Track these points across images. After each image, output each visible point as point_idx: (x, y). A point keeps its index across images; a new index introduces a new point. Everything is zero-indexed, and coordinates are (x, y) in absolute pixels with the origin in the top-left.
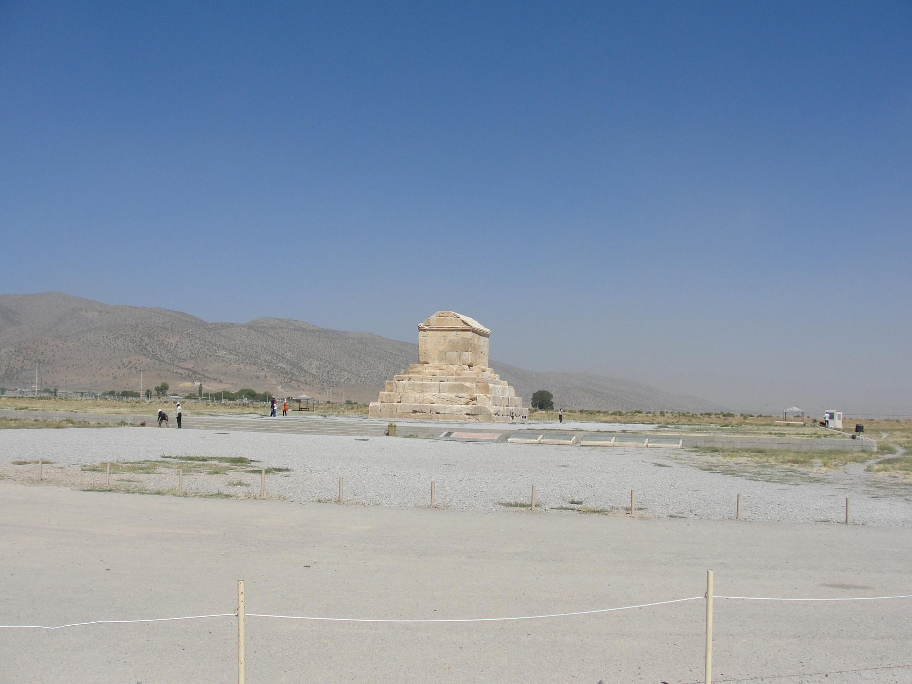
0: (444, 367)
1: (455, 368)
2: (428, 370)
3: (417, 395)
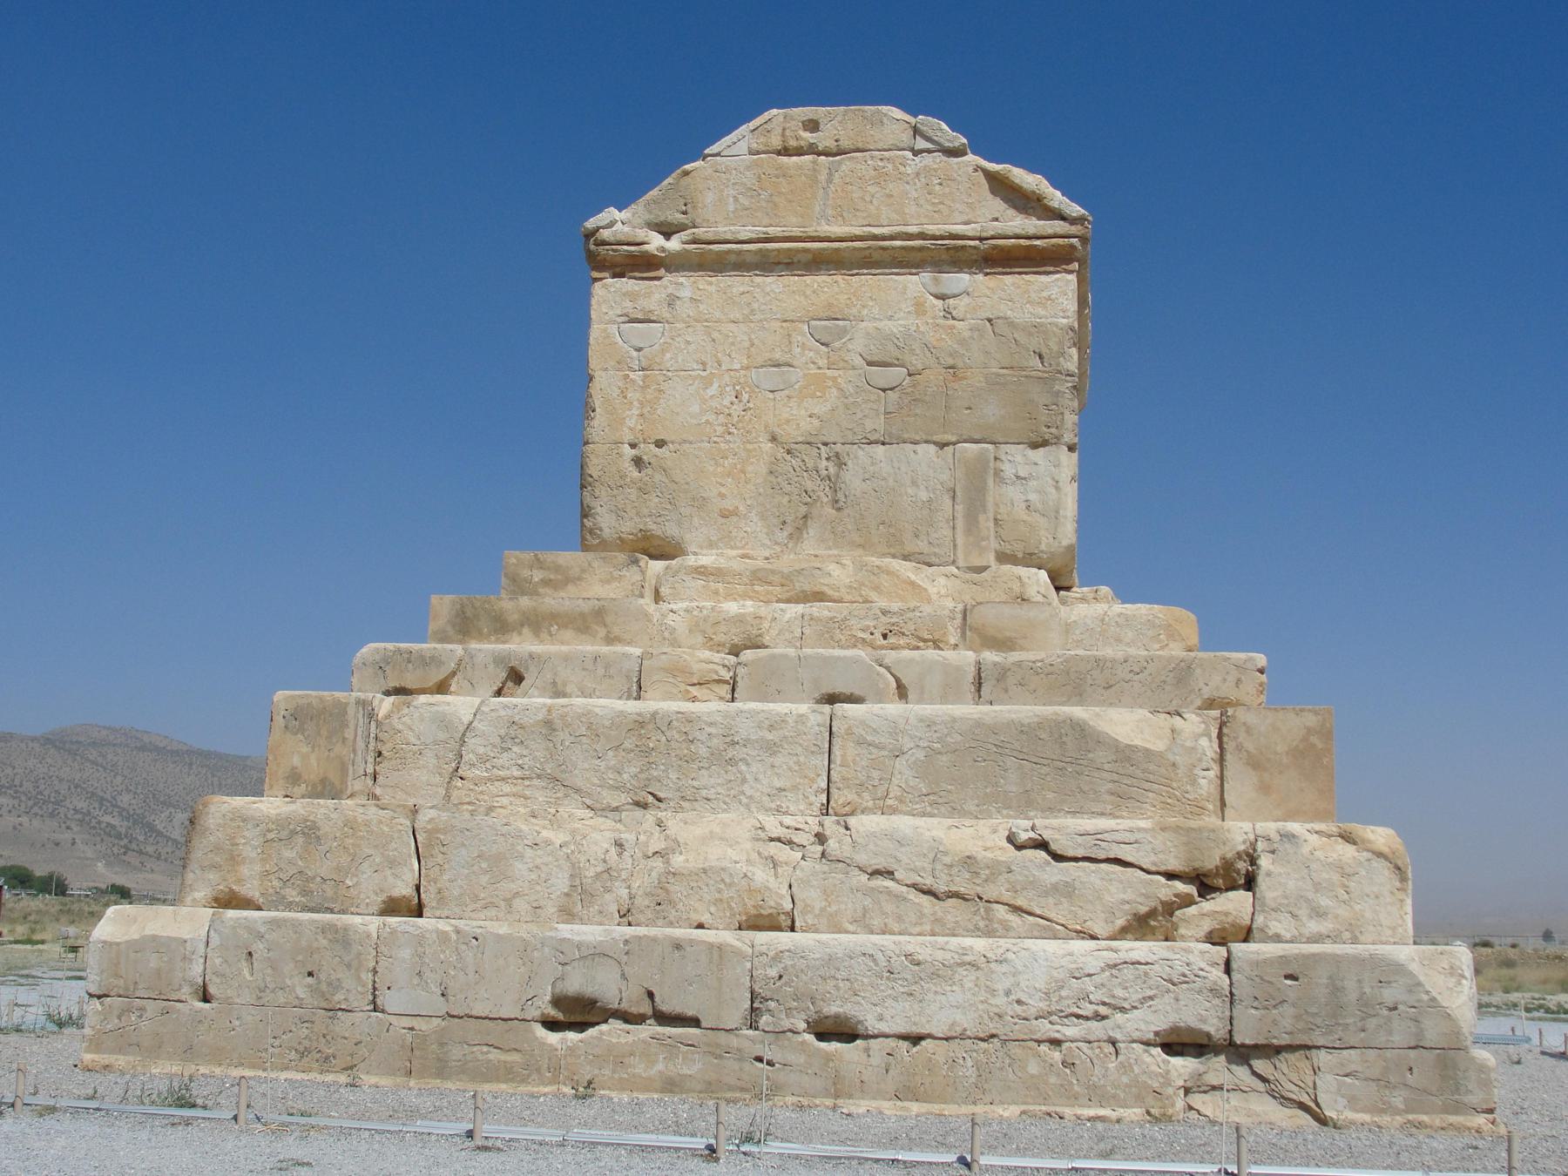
0: (839, 573)
1: (941, 590)
2: (683, 607)
3: (599, 835)
